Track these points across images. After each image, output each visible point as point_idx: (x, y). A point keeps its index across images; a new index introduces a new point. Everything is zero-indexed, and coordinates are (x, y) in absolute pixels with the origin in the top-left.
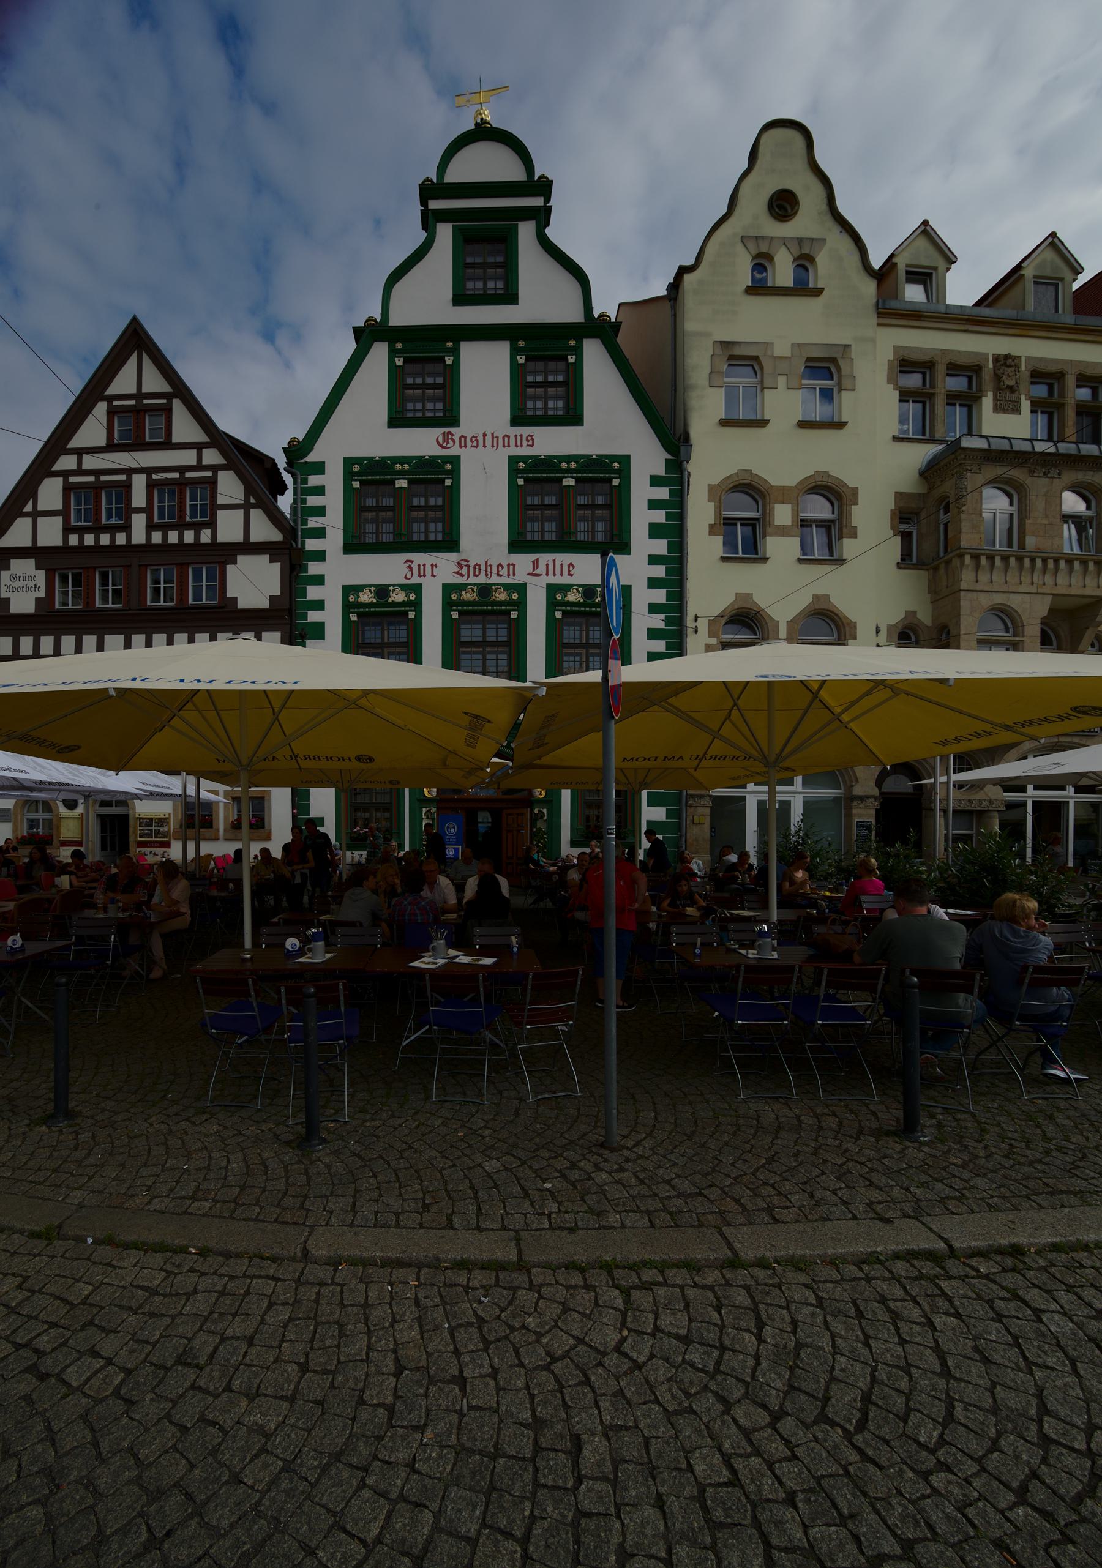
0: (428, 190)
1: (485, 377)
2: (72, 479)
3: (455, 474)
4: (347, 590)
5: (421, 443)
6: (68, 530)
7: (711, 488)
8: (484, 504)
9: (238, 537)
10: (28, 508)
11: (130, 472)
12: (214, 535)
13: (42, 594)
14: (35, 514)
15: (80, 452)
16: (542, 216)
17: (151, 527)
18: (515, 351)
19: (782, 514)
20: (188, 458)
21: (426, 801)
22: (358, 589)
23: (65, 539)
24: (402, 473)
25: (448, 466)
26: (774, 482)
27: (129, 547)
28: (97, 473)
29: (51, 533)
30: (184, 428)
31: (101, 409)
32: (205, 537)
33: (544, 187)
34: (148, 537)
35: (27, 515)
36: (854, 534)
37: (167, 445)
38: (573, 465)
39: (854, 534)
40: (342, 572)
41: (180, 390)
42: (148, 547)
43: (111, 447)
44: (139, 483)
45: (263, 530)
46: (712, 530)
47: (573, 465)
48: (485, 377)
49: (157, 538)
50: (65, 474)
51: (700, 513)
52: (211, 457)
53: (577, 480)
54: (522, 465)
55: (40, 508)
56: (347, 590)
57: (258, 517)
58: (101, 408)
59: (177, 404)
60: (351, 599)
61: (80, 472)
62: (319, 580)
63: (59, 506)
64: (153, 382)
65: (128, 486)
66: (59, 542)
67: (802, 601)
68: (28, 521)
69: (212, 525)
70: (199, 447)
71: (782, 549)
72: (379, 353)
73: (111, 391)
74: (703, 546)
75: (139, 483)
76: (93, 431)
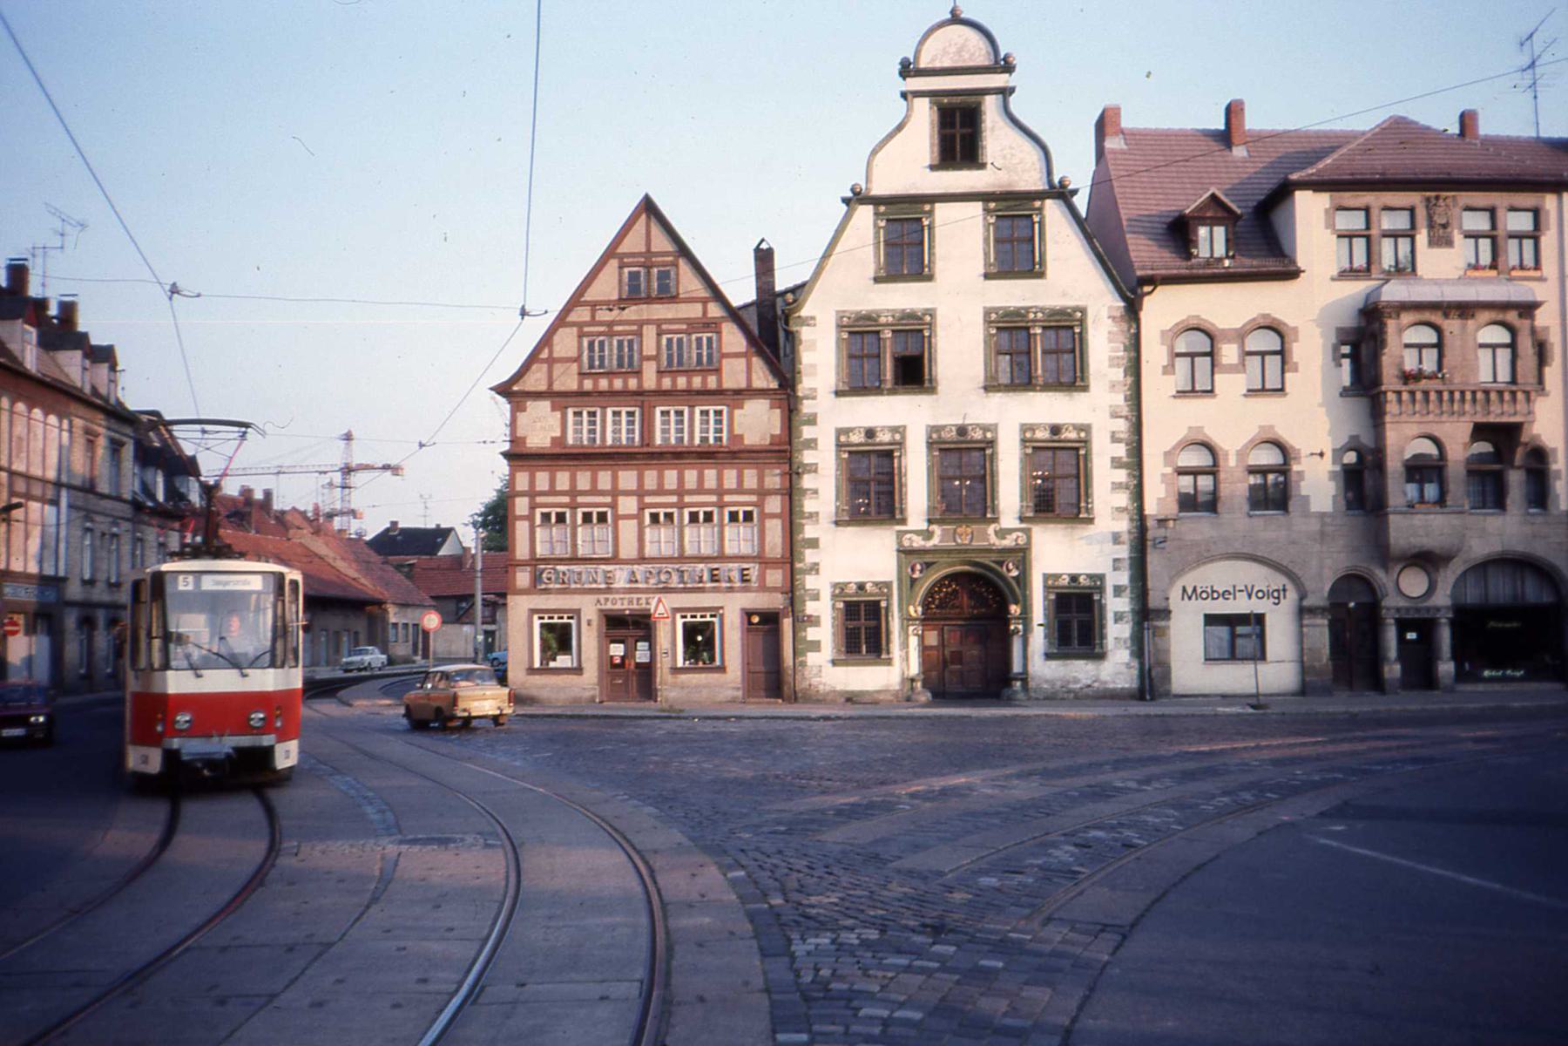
0: (907, 70)
1: (960, 236)
2: (586, 329)
3: (931, 325)
4: (840, 432)
5: (902, 297)
6: (582, 375)
7: (1163, 333)
8: (959, 352)
9: (743, 385)
10: (545, 354)
11: (641, 323)
12: (720, 381)
13: (558, 434)
14: (551, 361)
15: (594, 305)
16: (1005, 92)
17: (661, 373)
18: (987, 211)
19: (1229, 353)
20: (695, 311)
21: (910, 619)
22: (847, 431)
23: (581, 384)
24: (887, 325)
25: (928, 318)
26: (1221, 326)
27: (640, 393)
28: (611, 324)
29: (567, 380)
30: (688, 283)
31: (614, 263)
32: (712, 382)
33: (1007, 67)
34: (659, 381)
35: (543, 361)
36: (1296, 370)
37: (674, 299)
38: (1040, 315)
39: (1296, 370)
40: (834, 416)
41: (683, 251)
42: (660, 393)
43: (622, 303)
44: (650, 332)
45: (762, 378)
46: (1169, 369)
47: (1040, 315)
48: (960, 236)
49: (667, 383)
50: (580, 325)
51: (1154, 354)
52: (715, 310)
53: (1044, 328)
54: (994, 316)
55: (555, 355)
56: (840, 432)
57: (757, 362)
58: (614, 263)
59: (682, 262)
60: (843, 439)
61: (593, 322)
62: (812, 420)
63: (574, 354)
64: (661, 243)
65: (639, 334)
66: (574, 386)
67: (1250, 432)
68: (545, 367)
69: (718, 371)
70: (704, 302)
71: (1231, 385)
72: (865, 213)
73: (621, 250)
74: (1158, 386)
75: (650, 332)
76: (608, 286)
